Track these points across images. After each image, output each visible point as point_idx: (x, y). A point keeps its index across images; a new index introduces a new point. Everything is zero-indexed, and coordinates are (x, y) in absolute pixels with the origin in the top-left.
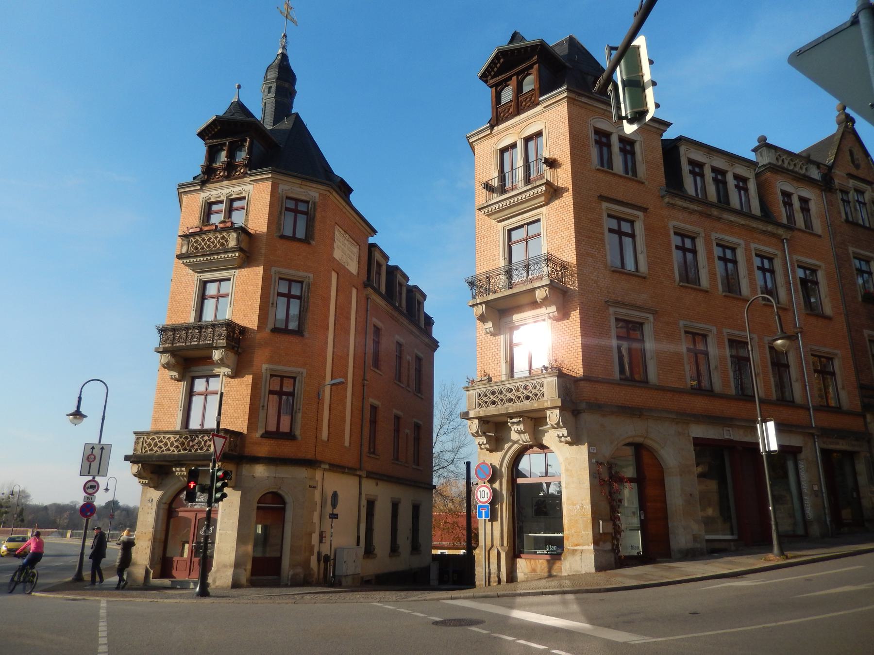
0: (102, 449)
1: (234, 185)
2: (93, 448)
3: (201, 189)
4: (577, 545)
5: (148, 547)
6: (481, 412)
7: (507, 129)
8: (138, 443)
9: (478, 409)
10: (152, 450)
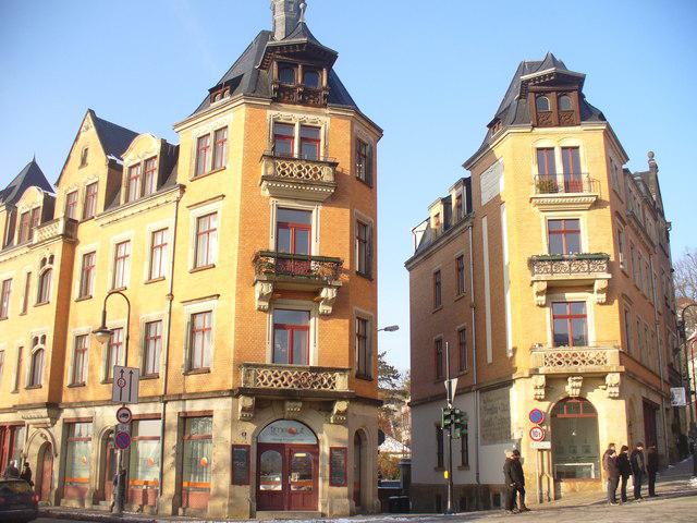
0: (131, 372)
1: (309, 112)
2: (122, 371)
3: (270, 108)
7: (547, 134)
10: (286, 385)
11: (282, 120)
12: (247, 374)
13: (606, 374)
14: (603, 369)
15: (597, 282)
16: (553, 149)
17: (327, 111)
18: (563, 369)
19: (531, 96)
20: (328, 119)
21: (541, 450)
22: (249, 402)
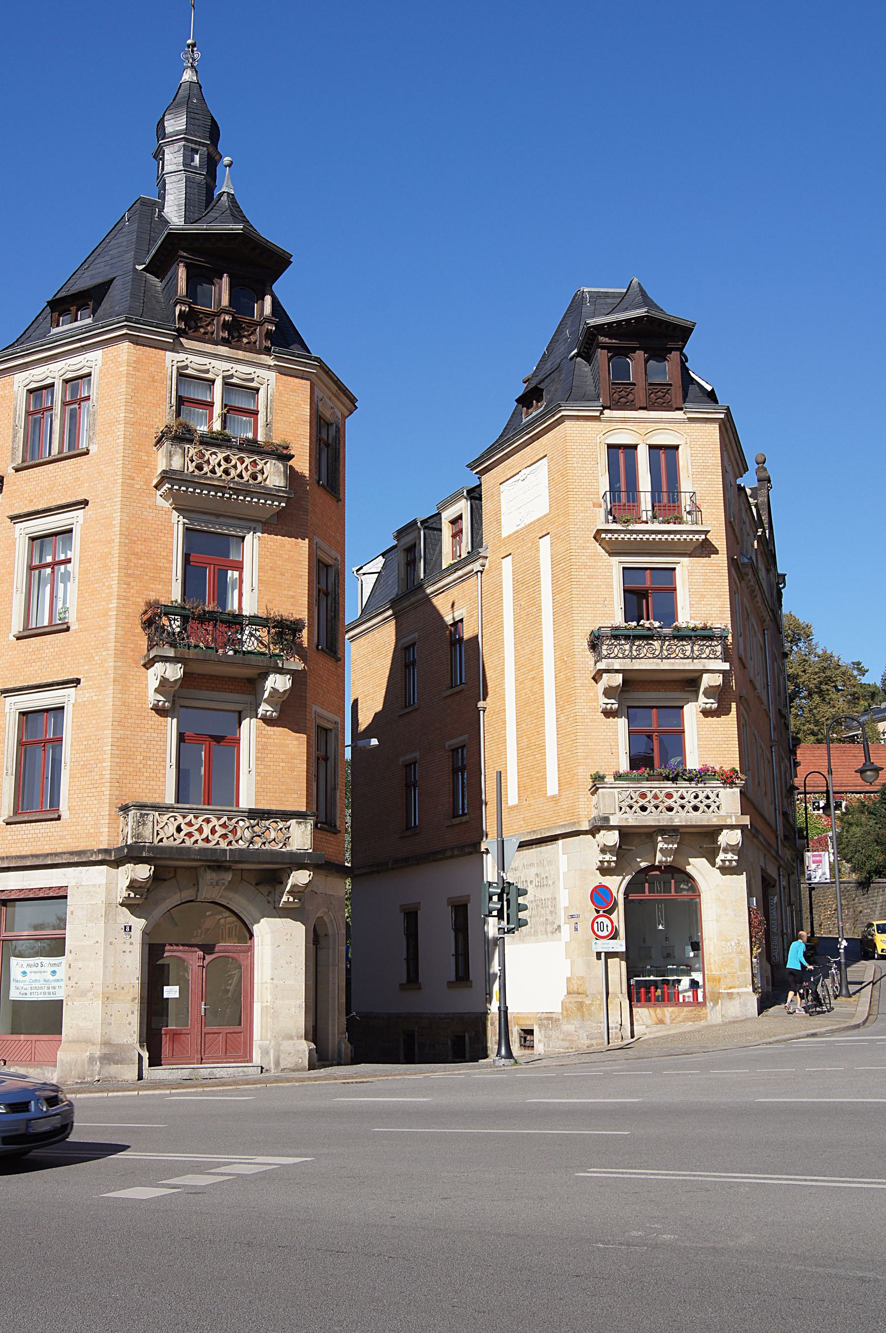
4: (731, 988)
5: (133, 1013)
7: (624, 420)
8: (144, 824)
9: (619, 814)
11: (189, 371)
12: (141, 822)
13: (719, 829)
14: (715, 821)
15: (705, 676)
16: (635, 447)
17: (270, 361)
18: (651, 819)
19: (601, 355)
20: (272, 375)
21: (609, 955)
22: (143, 872)
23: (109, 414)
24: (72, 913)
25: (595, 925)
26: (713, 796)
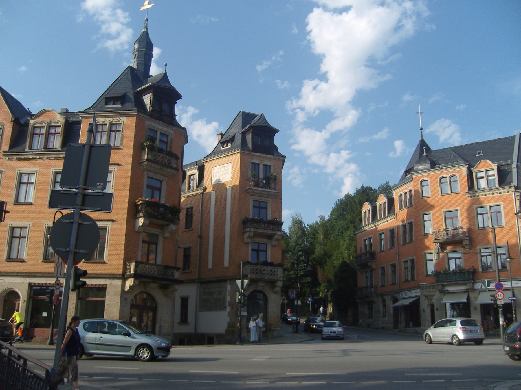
6: (253, 276)
7: (257, 156)
14: (276, 278)
18: (258, 276)
23: (128, 138)
24: (108, 293)
25: (503, 296)
26: (276, 271)
